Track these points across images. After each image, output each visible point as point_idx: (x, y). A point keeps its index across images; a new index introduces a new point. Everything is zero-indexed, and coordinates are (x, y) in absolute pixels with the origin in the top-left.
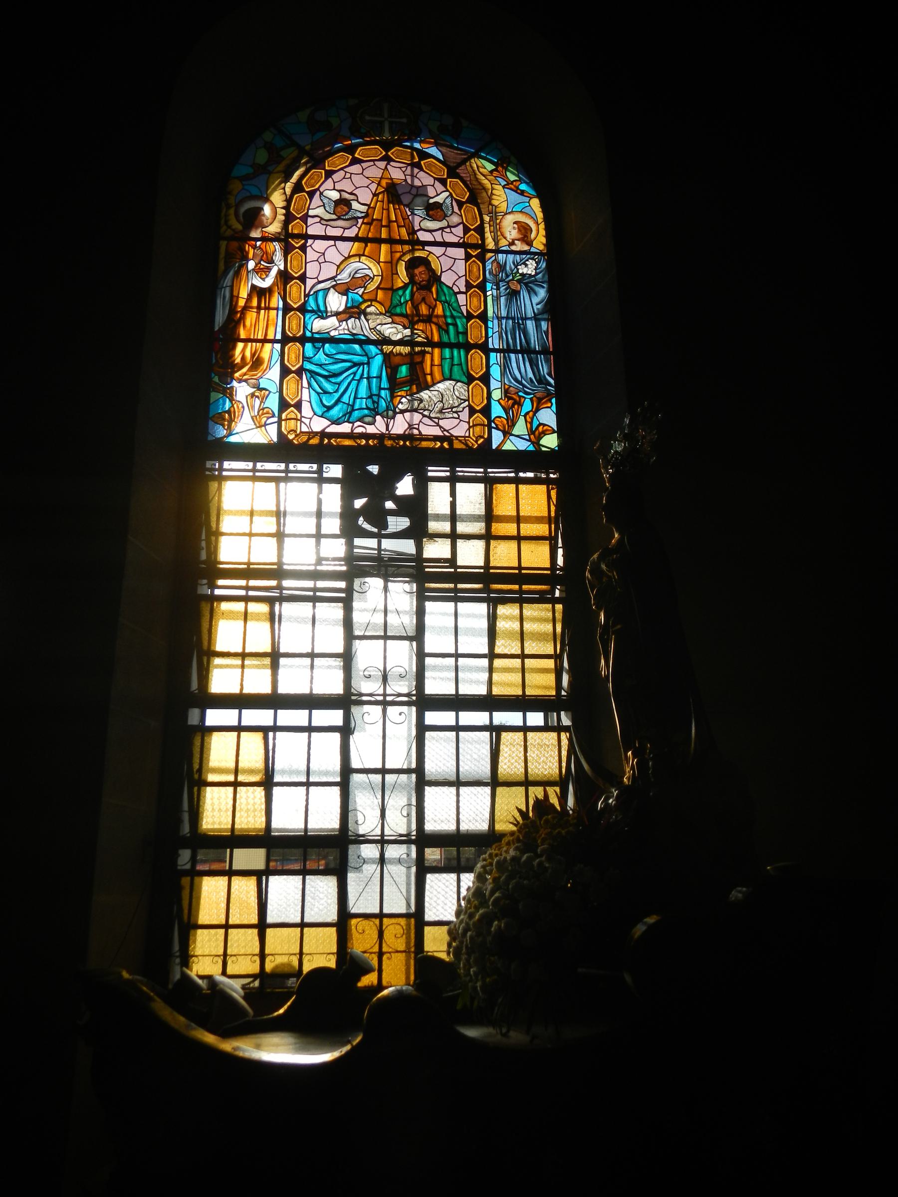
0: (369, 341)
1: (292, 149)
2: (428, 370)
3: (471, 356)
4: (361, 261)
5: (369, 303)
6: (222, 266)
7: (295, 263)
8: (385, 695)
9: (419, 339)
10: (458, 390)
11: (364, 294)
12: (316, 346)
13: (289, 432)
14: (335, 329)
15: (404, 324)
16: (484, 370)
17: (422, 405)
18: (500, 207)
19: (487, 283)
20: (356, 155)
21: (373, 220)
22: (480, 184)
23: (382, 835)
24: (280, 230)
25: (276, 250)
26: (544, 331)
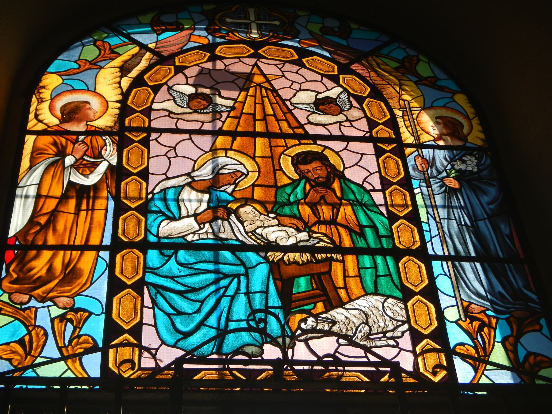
0: (244, 247)
1: (132, 46)
2: (340, 283)
4: (228, 155)
5: (243, 203)
6: (25, 162)
7: (133, 158)
9: (322, 244)
11: (235, 192)
12: (166, 254)
14: (194, 233)
15: (297, 227)
19: (412, 180)
24: (112, 124)
25: (105, 144)
26: (507, 236)
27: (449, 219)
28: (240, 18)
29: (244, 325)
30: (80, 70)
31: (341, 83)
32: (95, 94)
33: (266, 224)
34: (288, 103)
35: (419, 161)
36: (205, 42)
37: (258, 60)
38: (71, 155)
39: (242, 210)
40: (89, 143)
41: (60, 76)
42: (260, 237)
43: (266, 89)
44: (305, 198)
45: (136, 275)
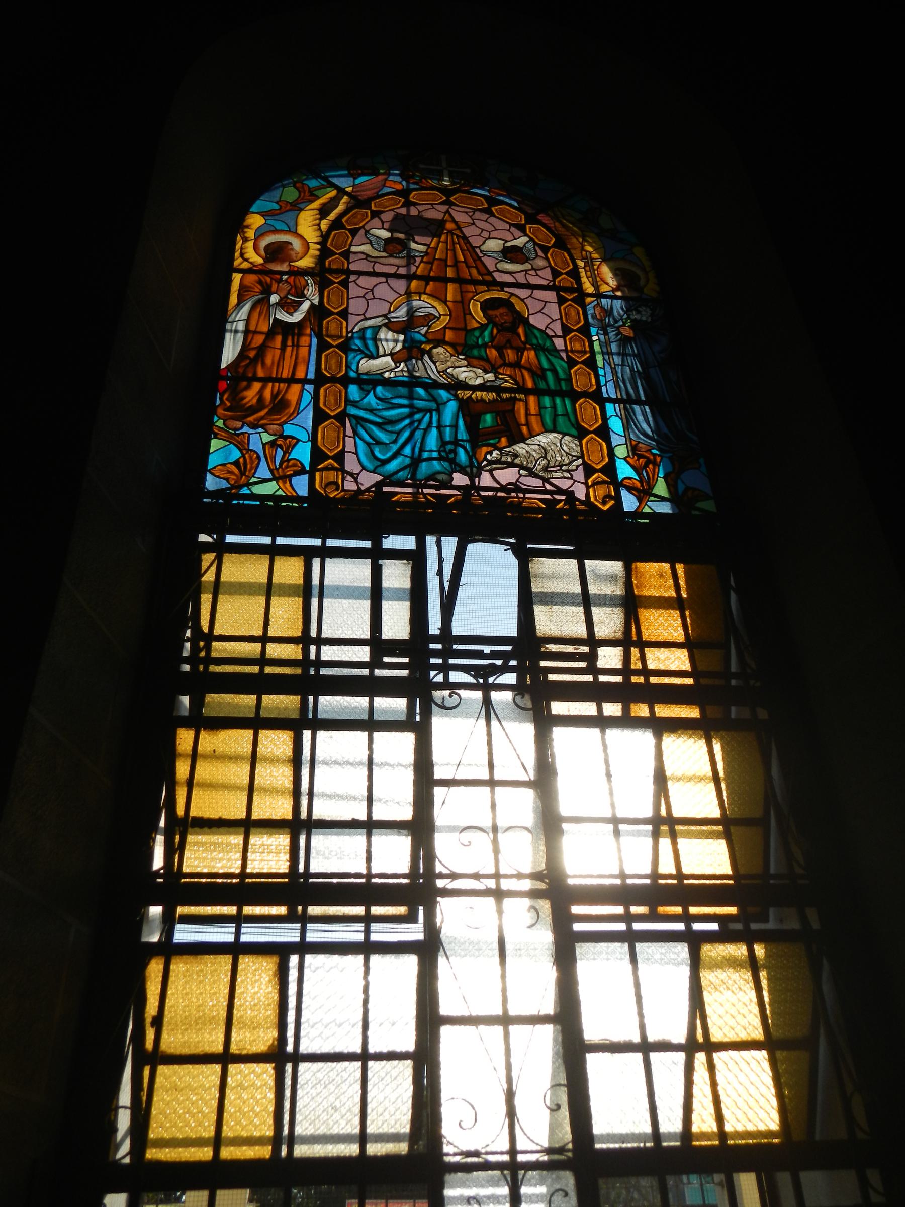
0: (436, 385)
3: (580, 405)
6: (234, 299)
7: (333, 298)
8: (497, 876)
9: (507, 384)
10: (567, 445)
14: (391, 371)
17: (517, 461)
23: (513, 1151)
27: (623, 365)
29: (435, 454)
30: (281, 212)
31: (528, 232)
33: (457, 364)
34: (478, 251)
35: (598, 309)
36: (399, 187)
37: (450, 207)
38: (276, 293)
39: (435, 351)
40: (292, 283)
41: (263, 216)
43: (458, 236)
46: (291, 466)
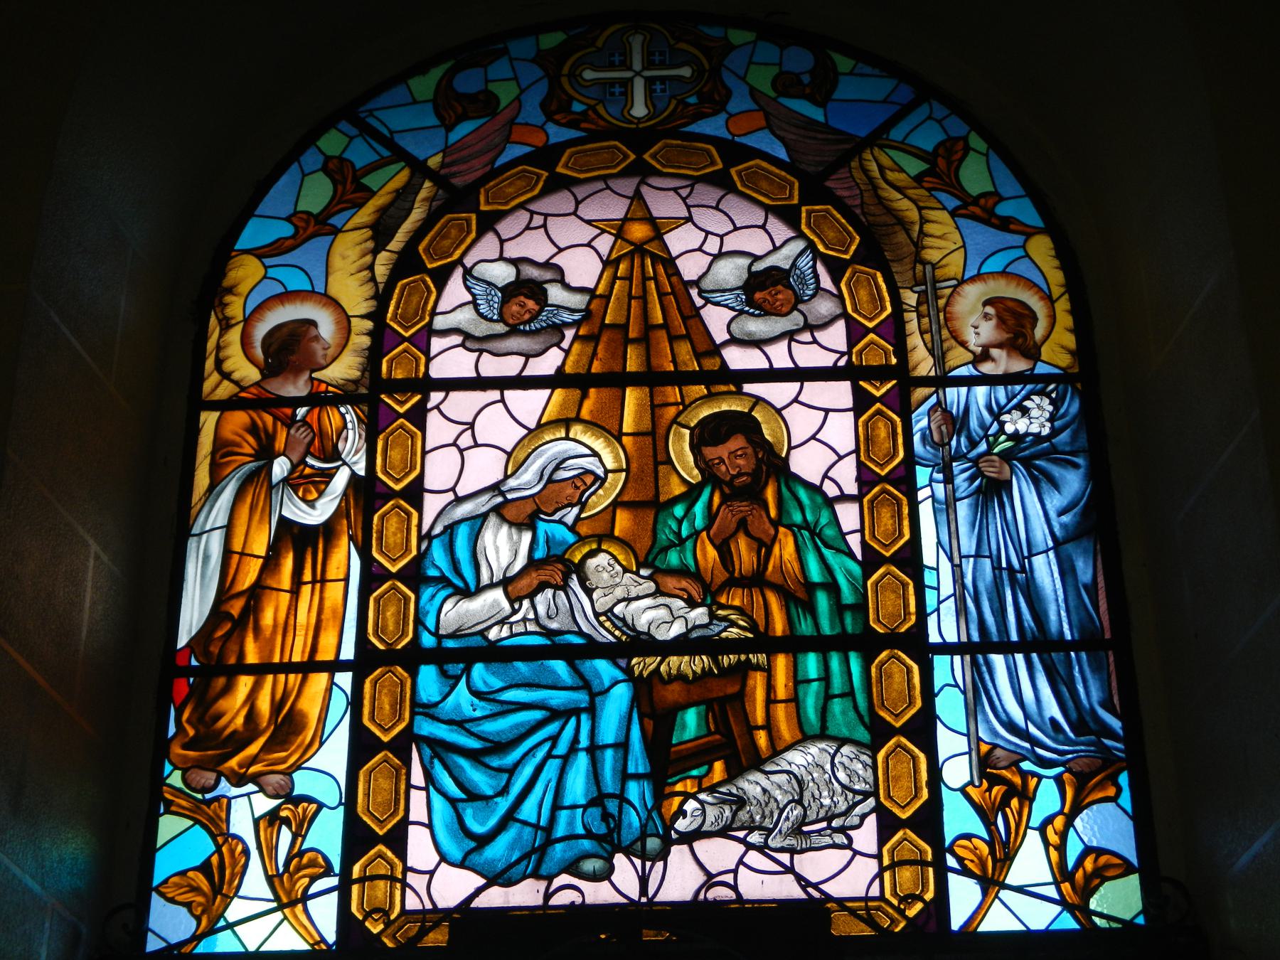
0: (593, 649)
2: (760, 717)
4: (571, 435)
5: (594, 546)
6: (202, 478)
7: (395, 455)
9: (734, 632)
10: (845, 768)
11: (580, 523)
13: (367, 915)
14: (502, 622)
15: (689, 595)
16: (919, 704)
17: (743, 816)
18: (945, 266)
19: (918, 468)
20: (560, 169)
21: (603, 326)
22: (890, 211)
24: (359, 374)
25: (345, 426)
26: (1085, 587)
27: (978, 555)
28: (611, 66)
30: (294, 243)
32: (325, 300)
36: (539, 140)
37: (642, 182)
39: (592, 563)
41: (260, 257)
42: (620, 624)
44: (707, 528)
45: (397, 721)
46: (307, 866)
